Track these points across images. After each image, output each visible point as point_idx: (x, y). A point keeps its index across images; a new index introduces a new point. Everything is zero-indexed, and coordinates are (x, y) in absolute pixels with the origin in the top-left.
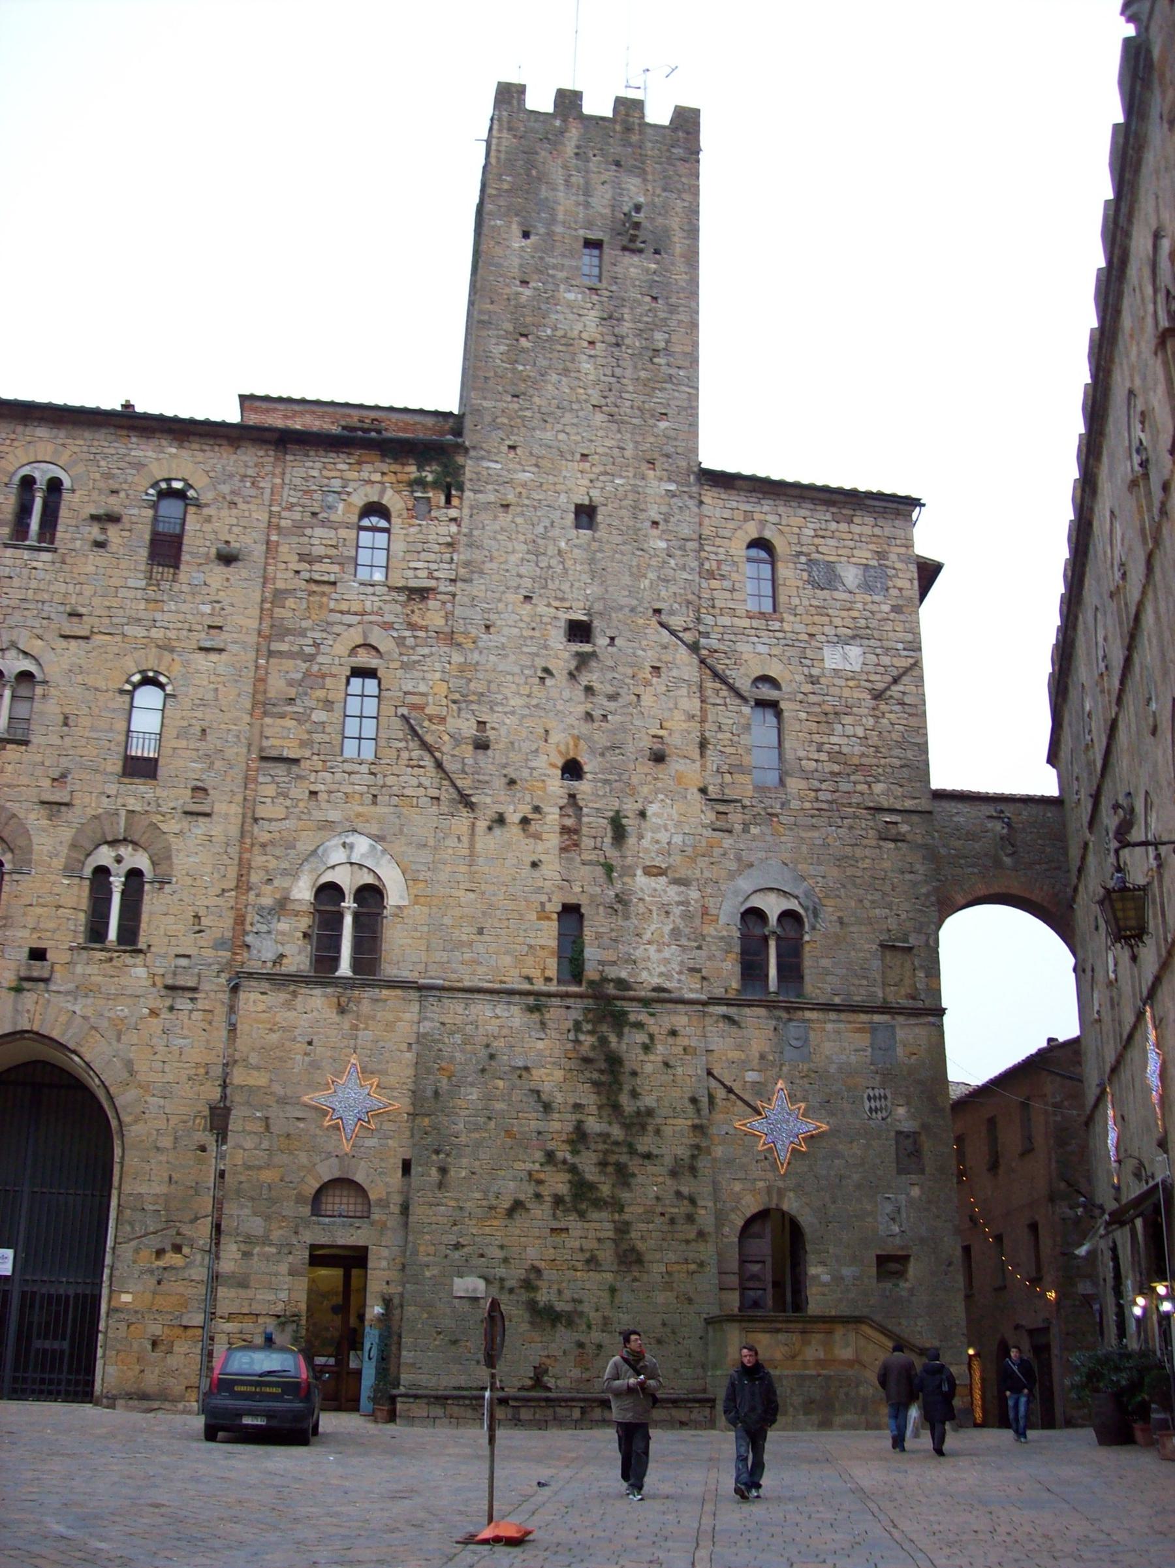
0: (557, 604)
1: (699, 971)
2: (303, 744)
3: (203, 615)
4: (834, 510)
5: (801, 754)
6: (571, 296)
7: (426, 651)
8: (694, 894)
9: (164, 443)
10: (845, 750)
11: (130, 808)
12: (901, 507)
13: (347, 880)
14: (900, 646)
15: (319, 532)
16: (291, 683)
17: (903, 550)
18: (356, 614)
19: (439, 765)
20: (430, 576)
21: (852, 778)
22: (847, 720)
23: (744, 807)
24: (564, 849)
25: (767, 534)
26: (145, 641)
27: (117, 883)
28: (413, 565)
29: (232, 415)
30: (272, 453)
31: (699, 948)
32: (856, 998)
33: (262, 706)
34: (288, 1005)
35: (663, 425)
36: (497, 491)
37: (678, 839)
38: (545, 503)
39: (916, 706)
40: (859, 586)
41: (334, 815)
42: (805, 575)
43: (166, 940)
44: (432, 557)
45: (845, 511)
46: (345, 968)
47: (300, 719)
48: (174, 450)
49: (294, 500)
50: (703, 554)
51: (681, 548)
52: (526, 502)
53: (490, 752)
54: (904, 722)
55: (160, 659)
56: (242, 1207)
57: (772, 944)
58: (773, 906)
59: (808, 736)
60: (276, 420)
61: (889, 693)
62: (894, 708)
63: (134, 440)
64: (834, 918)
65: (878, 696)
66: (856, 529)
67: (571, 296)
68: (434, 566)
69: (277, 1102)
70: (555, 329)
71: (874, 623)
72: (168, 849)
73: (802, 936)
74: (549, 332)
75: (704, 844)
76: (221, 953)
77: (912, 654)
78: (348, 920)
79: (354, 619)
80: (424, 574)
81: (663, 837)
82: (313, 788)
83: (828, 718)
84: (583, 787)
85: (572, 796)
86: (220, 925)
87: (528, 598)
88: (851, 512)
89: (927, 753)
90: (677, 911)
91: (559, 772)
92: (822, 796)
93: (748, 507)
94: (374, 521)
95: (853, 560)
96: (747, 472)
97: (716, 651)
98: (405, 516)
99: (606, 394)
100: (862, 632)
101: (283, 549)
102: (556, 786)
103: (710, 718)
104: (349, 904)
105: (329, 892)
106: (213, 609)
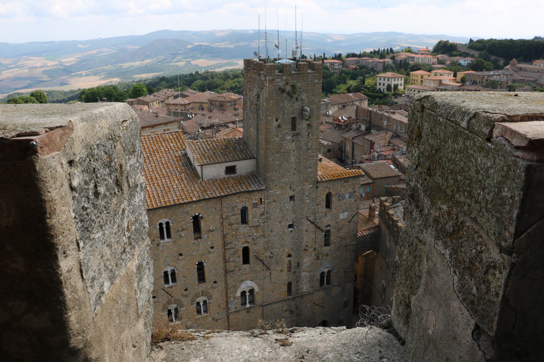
2: (235, 267)
6: (288, 138)
8: (312, 273)
15: (232, 217)
16: (231, 255)
19: (263, 263)
24: (288, 271)
25: (331, 191)
27: (201, 304)
33: (225, 261)
34: (238, 315)
35: (310, 170)
37: (309, 264)
41: (243, 278)
47: (233, 261)
51: (313, 201)
55: (201, 257)
58: (326, 270)
65: (349, 222)
66: (349, 183)
67: (288, 138)
70: (285, 149)
72: (211, 295)
79: (242, 236)
81: (307, 264)
83: (339, 230)
85: (290, 262)
86: (224, 305)
87: (280, 222)
93: (326, 185)
101: (224, 224)
102: (287, 260)
104: (248, 294)
105: (243, 294)
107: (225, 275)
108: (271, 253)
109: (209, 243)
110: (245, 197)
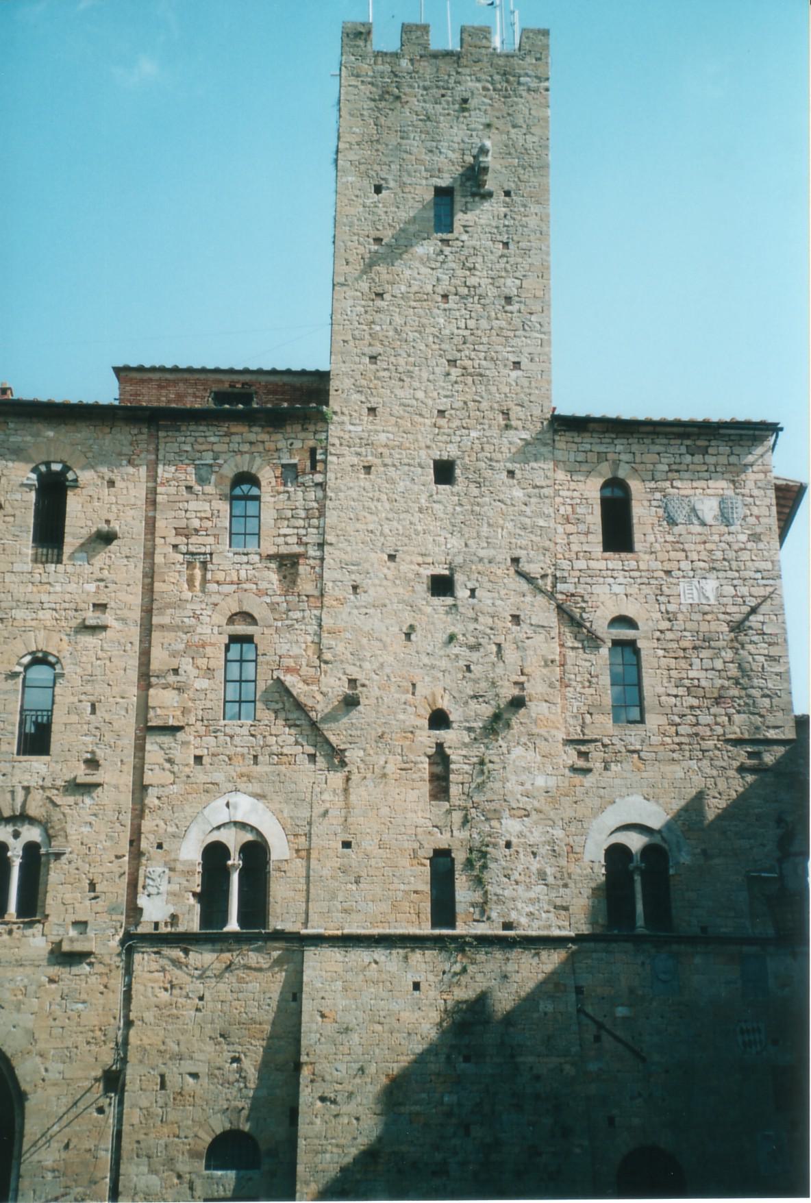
0: (420, 560)
1: (566, 909)
3: (88, 594)
4: (688, 442)
5: (661, 690)
7: (298, 615)
9: (40, 426)
10: (703, 683)
11: (26, 784)
12: (756, 433)
13: (233, 840)
14: (759, 575)
15: (193, 505)
16: (174, 655)
17: (761, 476)
18: (232, 583)
20: (300, 543)
21: (713, 710)
22: (705, 654)
23: (604, 746)
25: (621, 474)
26: (34, 623)
28: (283, 531)
29: (107, 392)
30: (145, 430)
31: (566, 886)
32: (723, 930)
35: (515, 374)
36: (358, 454)
38: (406, 461)
39: (776, 635)
40: (715, 518)
41: (219, 777)
42: (661, 511)
43: (63, 908)
44: (301, 523)
45: (699, 443)
46: (233, 925)
48: (51, 434)
49: (170, 476)
50: (558, 500)
52: (388, 461)
53: (360, 708)
54: (766, 652)
56: (138, 1165)
57: (637, 878)
59: (665, 672)
60: (150, 398)
61: (747, 623)
62: (754, 638)
63: (11, 425)
64: (699, 850)
66: (710, 460)
68: (303, 532)
69: (170, 1059)
71: (731, 555)
73: (667, 870)
74: (403, 288)
75: (567, 784)
76: (114, 917)
77: (771, 582)
78: (235, 878)
80: (294, 540)
82: (199, 753)
84: (449, 737)
85: (440, 746)
88: (706, 443)
89: (788, 681)
90: (544, 850)
91: (426, 723)
92: (682, 730)
93: (602, 449)
94: (245, 488)
95: (708, 491)
96: (597, 414)
97: (573, 595)
98: (274, 484)
99: (460, 347)
100: (718, 565)
102: (427, 739)
103: (569, 661)
104: (235, 860)
105: (215, 854)
106: (98, 587)
107: (140, 748)
108: (353, 682)
109: (91, 587)
110: (252, 437)
